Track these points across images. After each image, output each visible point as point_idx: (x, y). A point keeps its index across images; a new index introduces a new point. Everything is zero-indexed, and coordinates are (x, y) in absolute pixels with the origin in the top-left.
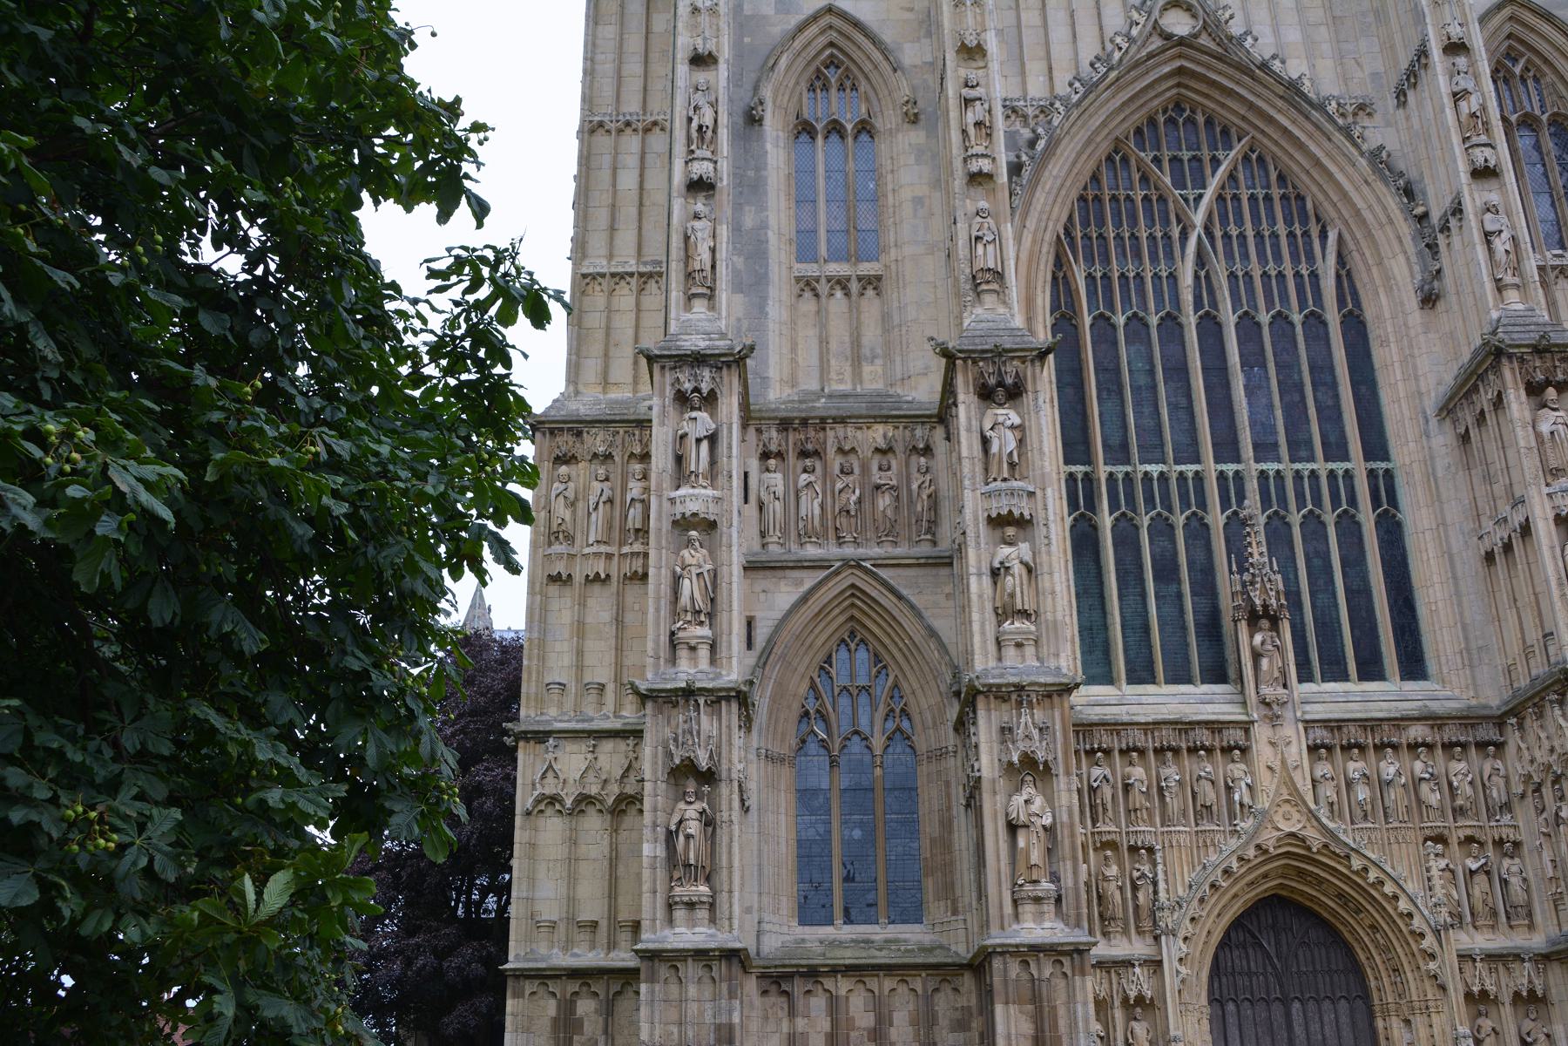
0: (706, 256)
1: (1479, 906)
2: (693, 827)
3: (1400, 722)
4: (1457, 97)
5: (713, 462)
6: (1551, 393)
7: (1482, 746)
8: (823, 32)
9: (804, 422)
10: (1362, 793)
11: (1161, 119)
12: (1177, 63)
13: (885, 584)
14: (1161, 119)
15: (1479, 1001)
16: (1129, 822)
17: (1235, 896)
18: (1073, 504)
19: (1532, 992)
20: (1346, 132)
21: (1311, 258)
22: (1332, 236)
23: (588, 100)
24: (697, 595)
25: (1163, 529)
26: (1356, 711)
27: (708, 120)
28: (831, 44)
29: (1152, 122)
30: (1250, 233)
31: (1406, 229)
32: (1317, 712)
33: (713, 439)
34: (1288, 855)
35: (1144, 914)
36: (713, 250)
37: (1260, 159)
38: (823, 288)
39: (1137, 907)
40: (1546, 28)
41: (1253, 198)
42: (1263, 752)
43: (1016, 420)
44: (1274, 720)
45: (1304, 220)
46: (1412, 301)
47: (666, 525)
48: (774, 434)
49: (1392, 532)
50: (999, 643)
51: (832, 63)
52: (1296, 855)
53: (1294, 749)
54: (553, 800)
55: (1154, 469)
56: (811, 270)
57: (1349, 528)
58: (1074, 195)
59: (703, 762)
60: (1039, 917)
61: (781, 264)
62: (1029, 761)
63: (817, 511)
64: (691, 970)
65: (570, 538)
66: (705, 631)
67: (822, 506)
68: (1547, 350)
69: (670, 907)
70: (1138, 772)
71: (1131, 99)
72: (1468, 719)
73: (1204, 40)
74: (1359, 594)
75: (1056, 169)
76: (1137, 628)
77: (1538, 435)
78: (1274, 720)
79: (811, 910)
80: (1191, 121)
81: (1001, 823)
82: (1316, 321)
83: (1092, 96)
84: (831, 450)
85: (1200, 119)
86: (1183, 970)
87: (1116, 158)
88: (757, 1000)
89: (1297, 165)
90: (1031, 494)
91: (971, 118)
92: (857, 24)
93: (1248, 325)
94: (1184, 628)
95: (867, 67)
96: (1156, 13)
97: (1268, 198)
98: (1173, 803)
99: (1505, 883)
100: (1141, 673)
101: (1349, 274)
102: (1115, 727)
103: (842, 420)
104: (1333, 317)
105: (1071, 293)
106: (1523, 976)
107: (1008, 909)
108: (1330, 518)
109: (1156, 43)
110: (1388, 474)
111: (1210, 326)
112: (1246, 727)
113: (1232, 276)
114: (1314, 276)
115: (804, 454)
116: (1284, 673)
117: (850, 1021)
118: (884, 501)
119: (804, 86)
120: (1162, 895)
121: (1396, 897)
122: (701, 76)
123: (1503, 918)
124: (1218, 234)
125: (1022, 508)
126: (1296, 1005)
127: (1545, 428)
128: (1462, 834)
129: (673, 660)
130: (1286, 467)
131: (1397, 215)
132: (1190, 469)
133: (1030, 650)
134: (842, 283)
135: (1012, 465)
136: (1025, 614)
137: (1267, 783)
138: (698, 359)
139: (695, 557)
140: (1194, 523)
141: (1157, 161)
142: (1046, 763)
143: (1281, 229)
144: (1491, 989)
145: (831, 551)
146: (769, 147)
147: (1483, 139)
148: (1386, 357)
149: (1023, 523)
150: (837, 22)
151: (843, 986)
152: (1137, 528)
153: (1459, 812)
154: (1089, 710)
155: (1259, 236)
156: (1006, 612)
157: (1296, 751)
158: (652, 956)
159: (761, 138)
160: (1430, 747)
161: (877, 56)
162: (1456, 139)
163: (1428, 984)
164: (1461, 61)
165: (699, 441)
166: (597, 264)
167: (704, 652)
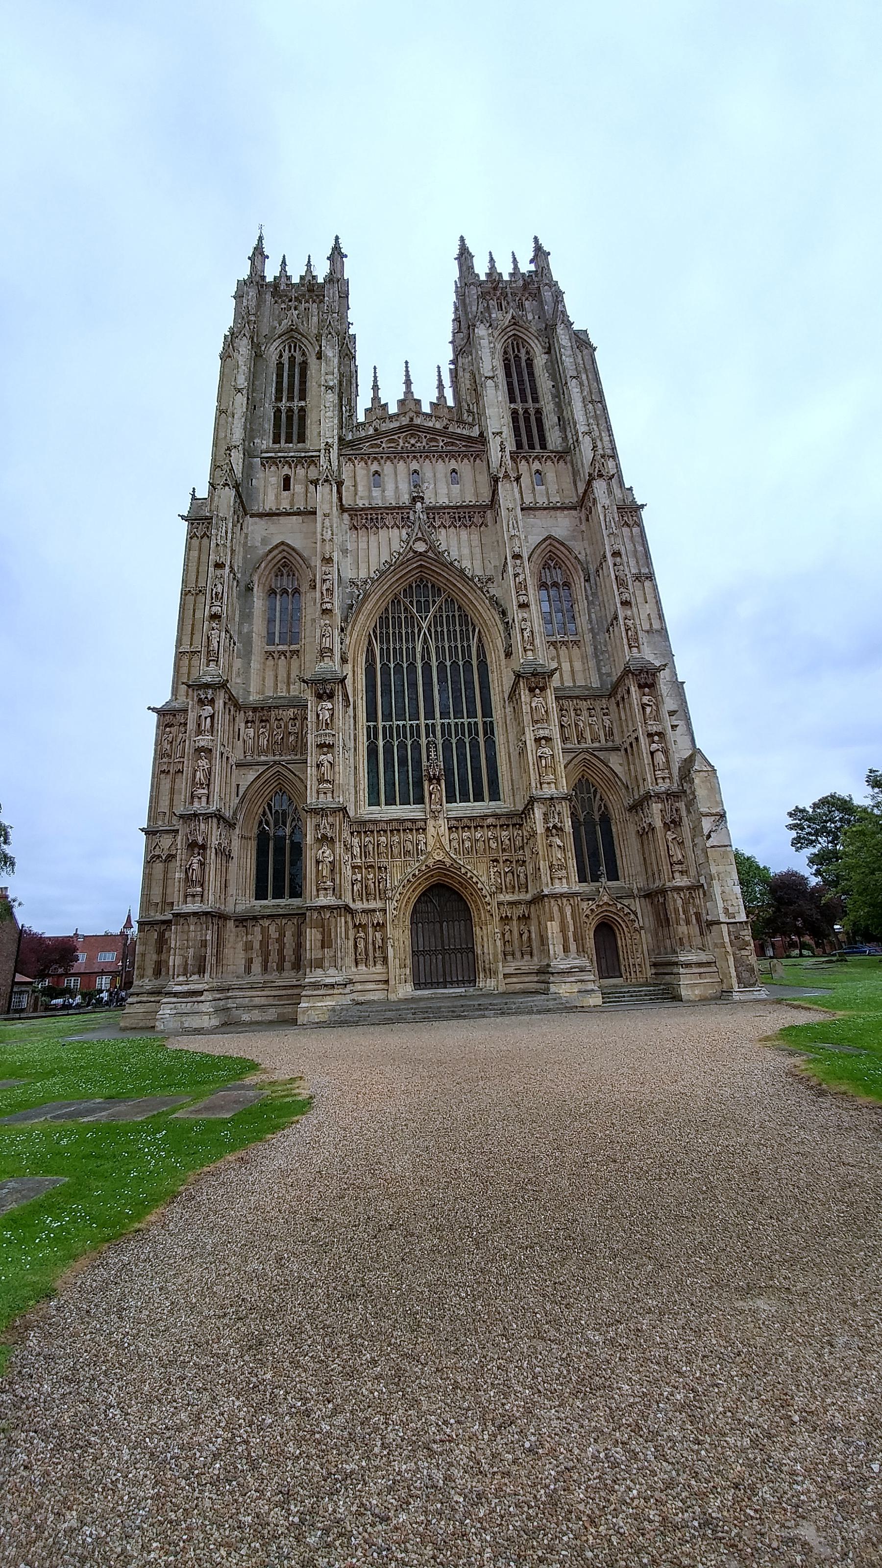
0: (216, 645)
1: (508, 885)
2: (195, 866)
3: (485, 817)
4: (516, 575)
5: (212, 726)
6: (537, 691)
7: (514, 825)
8: (280, 553)
9: (262, 708)
10: (467, 844)
11: (414, 585)
12: (419, 563)
13: (290, 770)
14: (414, 585)
15: (505, 920)
16: (378, 858)
17: (420, 884)
18: (369, 738)
19: (523, 915)
20: (481, 589)
21: (468, 639)
22: (477, 630)
23: (184, 582)
24: (202, 778)
25: (402, 746)
26: (468, 813)
27: (220, 590)
28: (285, 557)
29: (411, 586)
30: (445, 630)
31: (501, 627)
32: (453, 814)
33: (212, 717)
34: (438, 868)
35: (382, 892)
36: (219, 642)
37: (452, 600)
38: (276, 655)
39: (379, 890)
41: (448, 616)
42: (431, 830)
43: (330, 706)
44: (435, 818)
45: (467, 625)
47: (192, 751)
48: (251, 713)
49: (491, 744)
50: (318, 793)
51: (285, 565)
52: (441, 868)
53: (442, 828)
54: (159, 856)
55: (401, 723)
56: (271, 648)
57: (475, 745)
58: (377, 616)
59: (200, 842)
60: (326, 896)
61: (258, 644)
62: (325, 837)
63: (266, 742)
64: (192, 920)
65: (170, 756)
66: (206, 791)
67: (268, 741)
68: (537, 674)
69: (186, 896)
70: (383, 839)
71: (401, 577)
72: (509, 815)
73: (430, 554)
74: (476, 769)
75: (368, 606)
76: (390, 784)
77: (531, 707)
78: (435, 818)
79: (260, 894)
80: (426, 586)
81: (314, 861)
82: (468, 664)
84: (273, 720)
85: (430, 585)
86: (395, 912)
87: (395, 601)
88: (234, 930)
89: (464, 602)
90: (334, 735)
91: (324, 588)
92: (293, 549)
93: (441, 667)
94: (409, 784)
96: (411, 543)
97: (454, 616)
98: (396, 851)
99: (518, 876)
100: (390, 801)
101: (483, 646)
102: (375, 822)
103: (277, 707)
104: (475, 663)
105: (373, 655)
106: (521, 910)
107: (314, 893)
108: (467, 740)
109: (411, 554)
110: (491, 722)
111: (427, 667)
113: (437, 647)
114: (469, 646)
115: (262, 721)
116: (441, 799)
117: (269, 936)
118: (292, 738)
119: (273, 575)
120: (388, 885)
121: (477, 883)
122: (219, 572)
123: (517, 889)
124: (433, 630)
125: (329, 740)
126: (420, 925)
128: (504, 858)
129: (192, 803)
130: (452, 721)
131: (499, 622)
132: (414, 723)
134: (283, 653)
135: (327, 724)
136: (328, 781)
137: (431, 841)
138: (207, 686)
139: (203, 763)
140: (415, 743)
141: (411, 602)
142: (331, 838)
143: (458, 629)
144: (509, 915)
145: (271, 758)
146: (255, 599)
147: (524, 592)
148: (493, 677)
149: (331, 746)
150: (286, 548)
151: (266, 923)
152: (393, 746)
153: (504, 850)
154: (366, 816)
155: (449, 630)
156: (321, 780)
157: (444, 830)
158: (176, 915)
159: (252, 596)
160: (495, 826)
161: (301, 562)
162: (513, 592)
163: (487, 914)
164: (518, 562)
165: (206, 718)
166: (186, 648)
167: (204, 799)
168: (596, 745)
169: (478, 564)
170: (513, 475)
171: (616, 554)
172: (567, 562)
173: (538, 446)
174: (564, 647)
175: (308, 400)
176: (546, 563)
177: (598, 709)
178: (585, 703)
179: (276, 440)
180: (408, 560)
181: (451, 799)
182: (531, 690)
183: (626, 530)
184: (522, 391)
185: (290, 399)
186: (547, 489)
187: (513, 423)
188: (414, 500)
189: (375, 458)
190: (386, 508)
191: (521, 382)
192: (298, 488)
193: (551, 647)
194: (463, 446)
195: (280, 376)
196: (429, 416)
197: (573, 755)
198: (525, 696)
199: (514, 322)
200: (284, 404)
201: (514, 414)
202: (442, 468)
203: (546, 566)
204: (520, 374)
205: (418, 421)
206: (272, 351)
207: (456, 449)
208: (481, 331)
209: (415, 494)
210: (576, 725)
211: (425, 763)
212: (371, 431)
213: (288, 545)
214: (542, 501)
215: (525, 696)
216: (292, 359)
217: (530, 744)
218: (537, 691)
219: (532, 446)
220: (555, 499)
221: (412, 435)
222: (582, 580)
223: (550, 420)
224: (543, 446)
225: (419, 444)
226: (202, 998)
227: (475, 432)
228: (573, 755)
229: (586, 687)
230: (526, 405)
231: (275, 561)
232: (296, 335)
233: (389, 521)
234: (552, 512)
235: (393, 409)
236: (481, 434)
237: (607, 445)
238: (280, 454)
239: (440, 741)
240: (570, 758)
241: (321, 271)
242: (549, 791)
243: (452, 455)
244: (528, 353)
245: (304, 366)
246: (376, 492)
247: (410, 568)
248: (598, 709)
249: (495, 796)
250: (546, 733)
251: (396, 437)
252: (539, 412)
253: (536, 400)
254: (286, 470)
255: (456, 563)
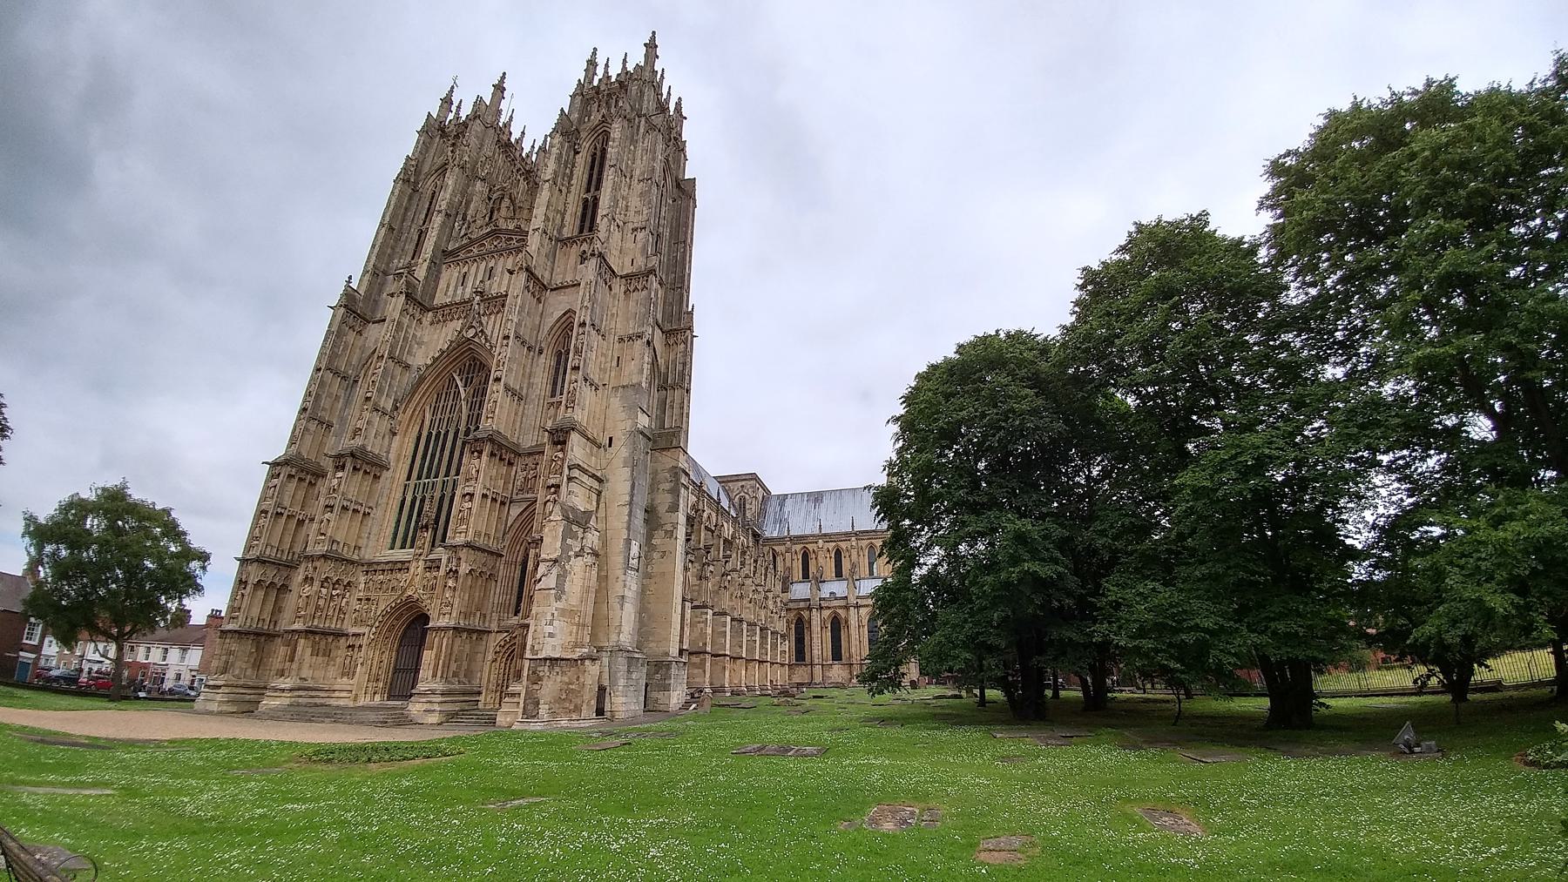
6: (476, 454)
83: (439, 361)
135: (334, 489)
226: (220, 691)
251: (484, 242)
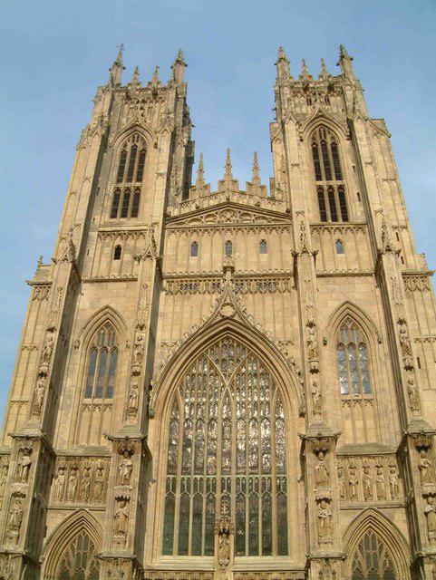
4: (309, 343)
6: (321, 454)
9: (74, 457)
25: (198, 499)
32: (240, 567)
33: (29, 466)
36: (42, 398)
40: (358, 312)
43: (129, 463)
46: (297, 414)
55: (198, 477)
57: (267, 501)
67: (76, 488)
73: (236, 318)
76: (184, 534)
78: (224, 571)
91: (136, 352)
95: (119, 327)
100: (183, 551)
103: (87, 457)
109: (219, 318)
112: (212, 572)
127: (317, 467)
133: (122, 545)
147: (315, 359)
150: (110, 311)
168: (383, 502)
169: (279, 326)
170: (311, 248)
171: (401, 322)
172: (363, 325)
173: (340, 219)
174: (357, 405)
175: (144, 181)
176: (344, 325)
177: (386, 466)
178: (373, 461)
179: (113, 216)
180: (215, 324)
181: (240, 549)
182: (317, 453)
183: (417, 294)
184: (328, 171)
185: (129, 180)
186: (346, 258)
187: (319, 197)
188: (225, 269)
189: (195, 231)
190: (200, 276)
191: (327, 163)
192: (126, 257)
193: (346, 406)
194: (274, 220)
195: (123, 162)
196: (243, 193)
197: (360, 512)
198: (310, 457)
199: (321, 115)
200: (123, 185)
201: (320, 190)
202: (253, 239)
203: (343, 327)
204: (326, 156)
205: (234, 199)
206: (117, 144)
207: (265, 222)
208: (291, 127)
209: (225, 265)
210: (364, 483)
211: (218, 517)
212: (194, 209)
213: (111, 309)
214: (342, 268)
215: (310, 457)
216: (134, 149)
217: (312, 505)
218: (321, 454)
219: (335, 219)
220: (354, 267)
221: (228, 210)
222: (376, 341)
223: (352, 191)
224: (345, 218)
225: (234, 218)
227: (282, 209)
228: (360, 512)
229: (375, 445)
230: (331, 183)
231: (100, 321)
232: (139, 129)
233: (202, 286)
234: (350, 279)
235: (214, 188)
236: (289, 211)
237: (401, 216)
238: (114, 229)
239: (233, 496)
240: (356, 515)
241: (165, 79)
242: (324, 551)
243: (262, 228)
244: (333, 138)
245: (143, 156)
246: (193, 260)
247: (218, 330)
248: (386, 466)
249: (283, 551)
250: (326, 494)
251: (214, 213)
252: (341, 187)
253: (339, 177)
254: (118, 242)
255: (258, 327)
